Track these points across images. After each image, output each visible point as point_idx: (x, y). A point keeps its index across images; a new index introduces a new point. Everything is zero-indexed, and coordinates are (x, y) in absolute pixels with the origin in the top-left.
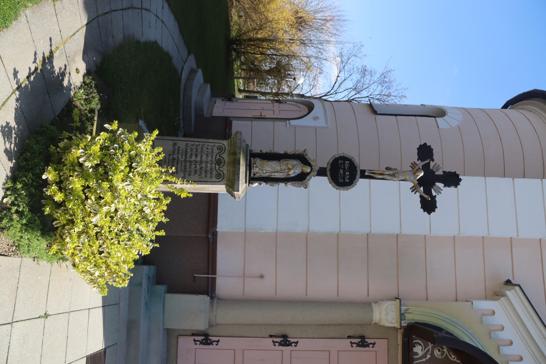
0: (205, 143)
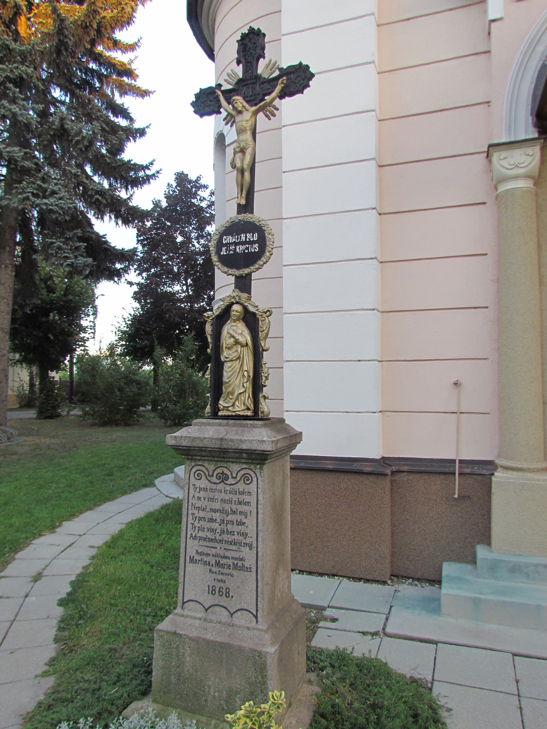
0: (190, 503)
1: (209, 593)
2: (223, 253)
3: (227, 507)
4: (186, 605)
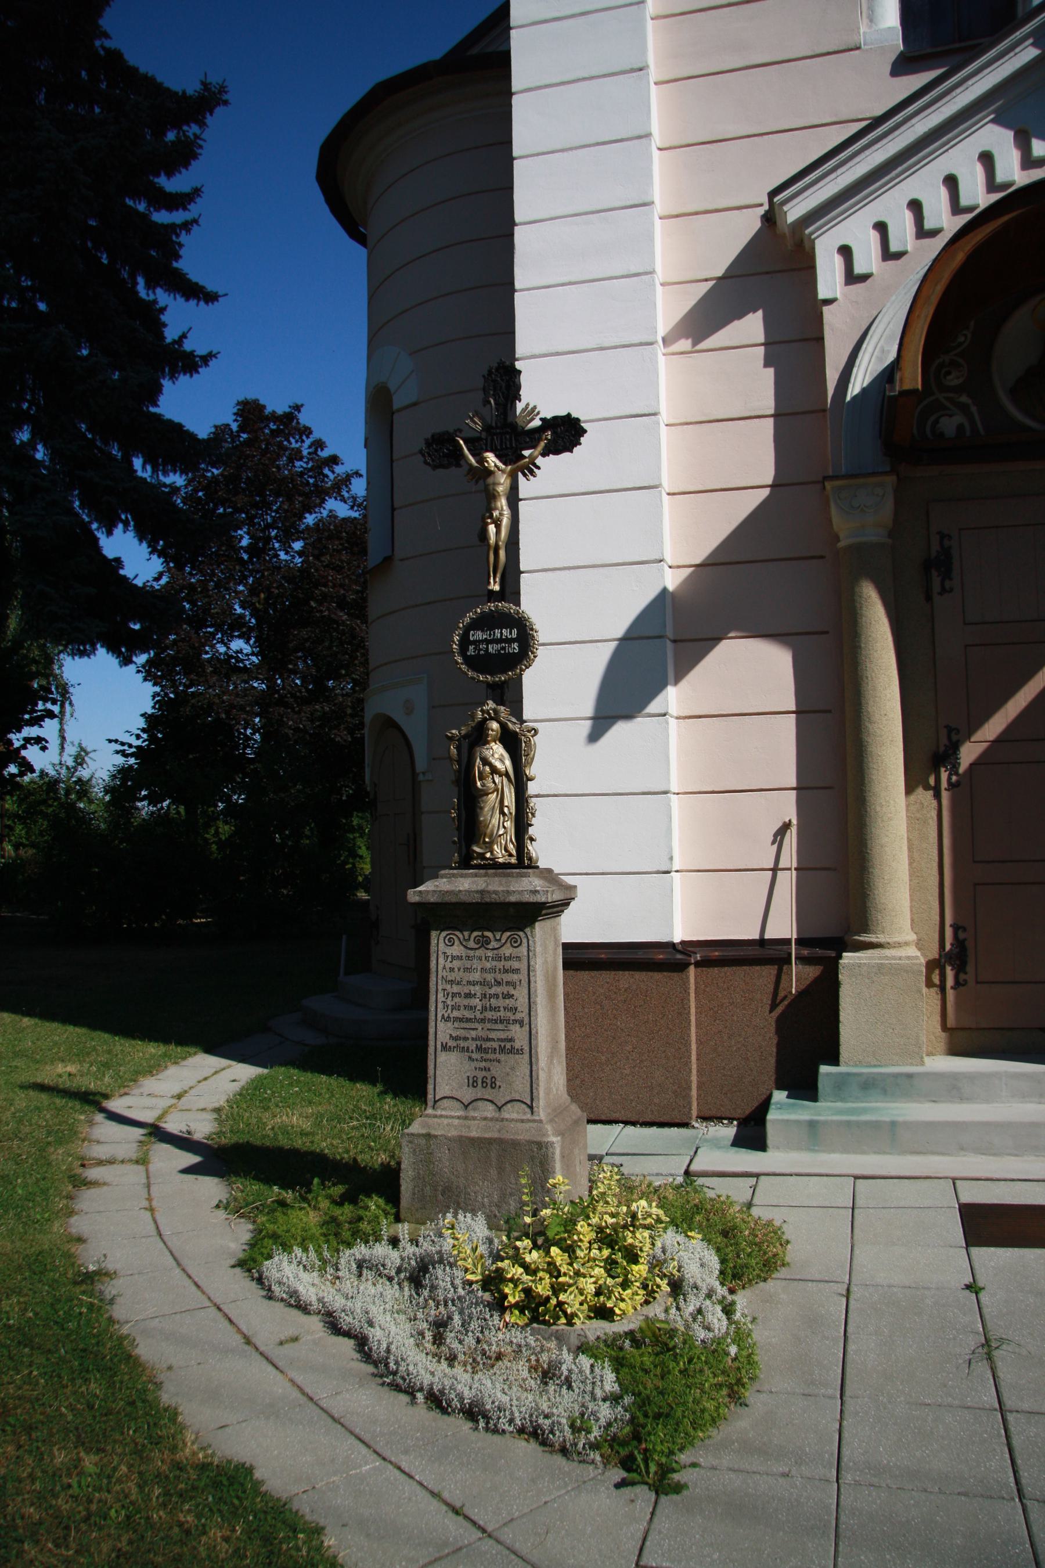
0: (440, 976)
1: (468, 1086)
2: (471, 651)
3: (489, 977)
4: (438, 1104)
